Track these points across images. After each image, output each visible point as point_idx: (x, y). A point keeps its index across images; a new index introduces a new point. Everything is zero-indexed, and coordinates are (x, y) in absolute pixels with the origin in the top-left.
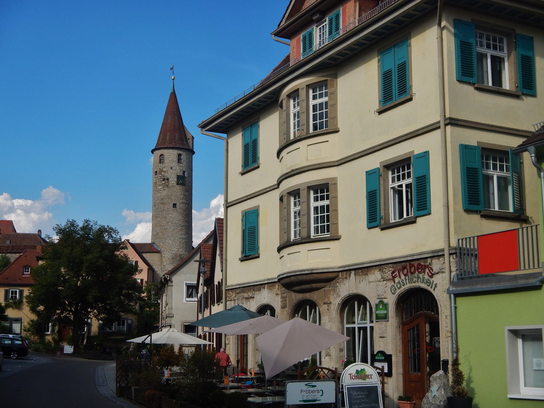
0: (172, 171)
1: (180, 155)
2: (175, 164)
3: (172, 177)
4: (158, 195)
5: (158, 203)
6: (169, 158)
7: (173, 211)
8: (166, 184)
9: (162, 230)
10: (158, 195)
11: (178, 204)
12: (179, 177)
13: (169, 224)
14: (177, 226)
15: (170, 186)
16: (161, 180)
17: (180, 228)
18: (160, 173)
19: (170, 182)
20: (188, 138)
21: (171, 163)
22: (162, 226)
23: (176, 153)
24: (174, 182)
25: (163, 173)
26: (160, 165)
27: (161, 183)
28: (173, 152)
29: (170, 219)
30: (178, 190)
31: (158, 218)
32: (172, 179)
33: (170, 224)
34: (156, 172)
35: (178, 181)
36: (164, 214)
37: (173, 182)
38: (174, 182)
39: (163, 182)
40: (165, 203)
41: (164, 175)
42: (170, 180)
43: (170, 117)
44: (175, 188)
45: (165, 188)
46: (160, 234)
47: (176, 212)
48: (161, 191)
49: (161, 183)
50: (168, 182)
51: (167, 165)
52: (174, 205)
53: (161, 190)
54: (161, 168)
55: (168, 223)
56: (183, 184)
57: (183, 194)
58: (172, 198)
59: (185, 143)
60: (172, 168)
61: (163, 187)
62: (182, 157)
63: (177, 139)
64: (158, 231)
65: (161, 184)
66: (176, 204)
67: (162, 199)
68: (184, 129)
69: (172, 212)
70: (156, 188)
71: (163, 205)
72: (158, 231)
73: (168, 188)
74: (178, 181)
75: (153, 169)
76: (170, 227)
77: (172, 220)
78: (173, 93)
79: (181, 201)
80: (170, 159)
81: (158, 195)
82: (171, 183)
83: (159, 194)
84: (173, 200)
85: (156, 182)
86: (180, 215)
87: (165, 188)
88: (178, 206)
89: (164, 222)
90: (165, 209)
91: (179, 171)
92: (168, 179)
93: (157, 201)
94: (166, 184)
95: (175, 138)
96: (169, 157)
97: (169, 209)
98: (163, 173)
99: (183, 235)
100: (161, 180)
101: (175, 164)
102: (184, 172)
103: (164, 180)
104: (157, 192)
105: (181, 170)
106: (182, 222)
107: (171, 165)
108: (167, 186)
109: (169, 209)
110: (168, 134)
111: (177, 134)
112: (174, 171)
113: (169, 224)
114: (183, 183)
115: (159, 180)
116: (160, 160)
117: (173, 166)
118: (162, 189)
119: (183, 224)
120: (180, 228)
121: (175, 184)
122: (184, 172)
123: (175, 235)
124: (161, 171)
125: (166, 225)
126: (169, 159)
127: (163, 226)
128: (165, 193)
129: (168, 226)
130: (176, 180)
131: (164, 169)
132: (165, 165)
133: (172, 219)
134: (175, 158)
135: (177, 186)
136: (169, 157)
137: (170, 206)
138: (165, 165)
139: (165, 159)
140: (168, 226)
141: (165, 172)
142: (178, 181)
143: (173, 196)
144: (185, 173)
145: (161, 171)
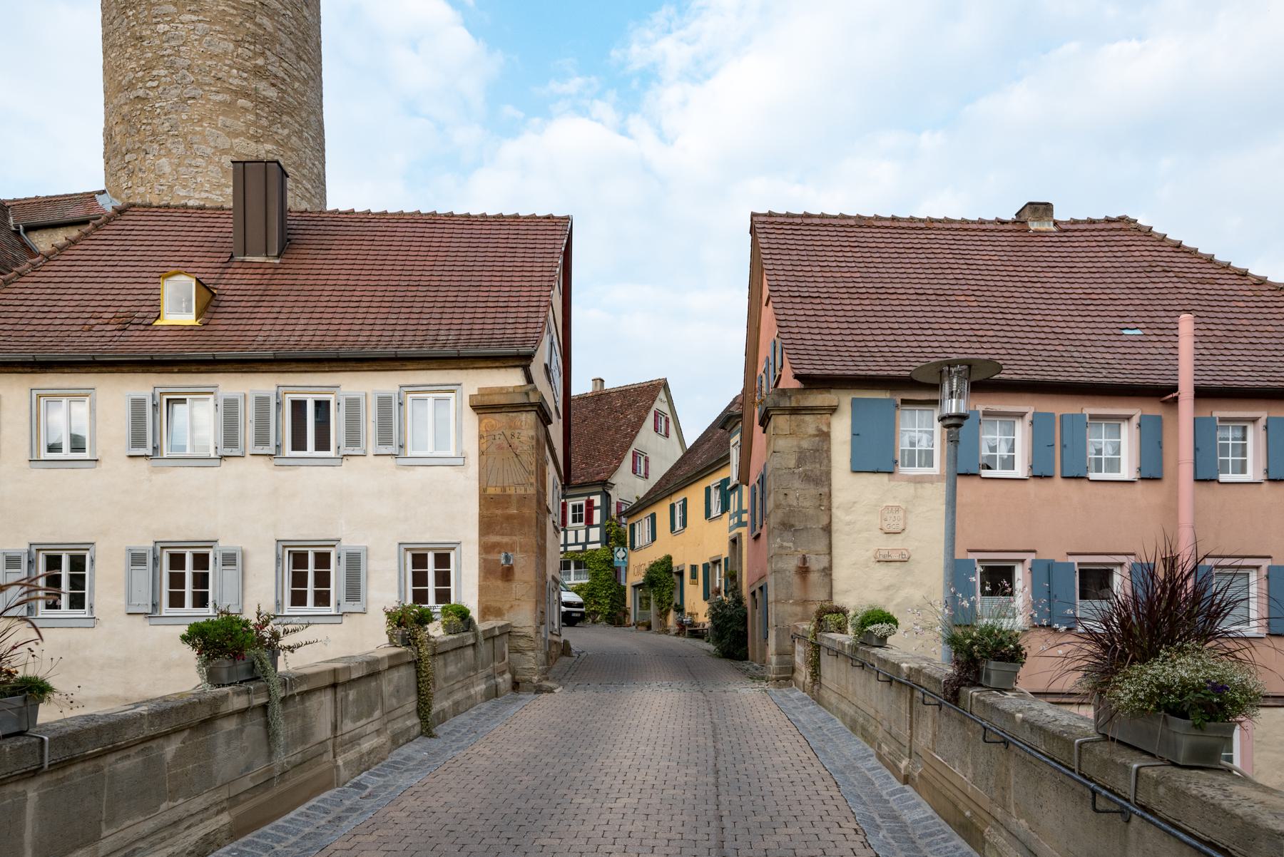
7: (175, 5)
9: (126, 109)
13: (155, 73)
14: (200, 85)
17: (219, 97)
29: (161, 48)
33: (163, 72)
46: (117, 129)
47: (192, 8)
55: (148, 68)
69: (172, 9)
76: (161, 89)
86: (218, 28)
89: (133, 65)
99: (237, 135)
106: (231, 67)
113: (155, 73)
119: (236, 82)
120: (219, 97)
123: (195, 133)
125: (142, 80)
127: (131, 86)
129: (150, 84)
133: (173, 43)
140: (150, 84)
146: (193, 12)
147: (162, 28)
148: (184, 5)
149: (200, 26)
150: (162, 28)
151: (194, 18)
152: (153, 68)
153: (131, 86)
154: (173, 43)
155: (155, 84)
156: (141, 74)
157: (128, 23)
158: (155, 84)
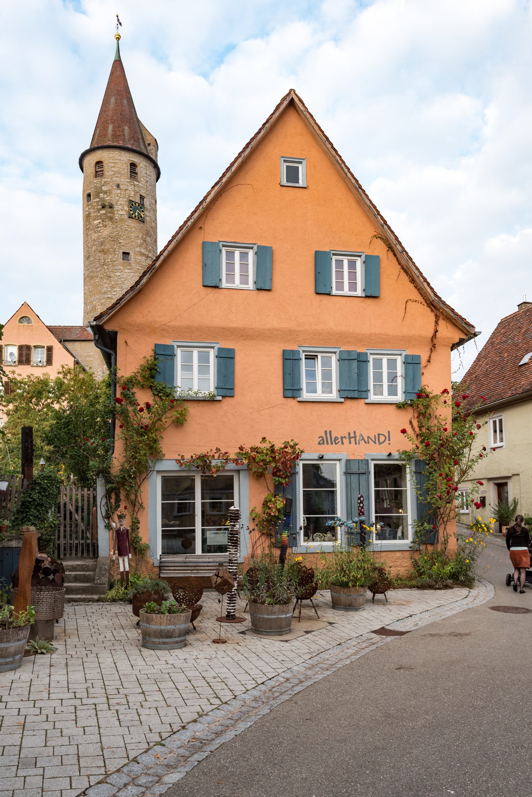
0: (119, 191)
1: (133, 165)
2: (124, 180)
3: (119, 203)
4: (94, 236)
5: (94, 252)
6: (113, 167)
8: (109, 215)
9: (103, 301)
10: (93, 237)
11: (132, 253)
12: (132, 205)
13: (115, 289)
15: (116, 219)
16: (99, 207)
18: (97, 196)
19: (116, 212)
20: (147, 143)
21: (117, 177)
22: (101, 293)
23: (125, 159)
24: (125, 213)
25: (101, 195)
26: (95, 181)
27: (99, 213)
28: (120, 157)
29: (118, 281)
30: (132, 229)
31: (95, 278)
32: (120, 207)
33: (118, 290)
34: (89, 195)
35: (131, 210)
36: (105, 270)
37: (121, 212)
38: (125, 213)
39: (103, 212)
40: (108, 251)
41: (103, 198)
42: (116, 207)
43: (113, 100)
44: (127, 223)
45: (107, 223)
46: (99, 307)
47: (129, 267)
48: (99, 229)
49: (99, 213)
50: (113, 213)
51: (109, 180)
52: (126, 254)
53: (98, 227)
54: (99, 185)
55: (113, 287)
56: (142, 220)
57: (140, 236)
58: (120, 241)
59: (142, 146)
60: (118, 186)
61: (103, 221)
62: (138, 170)
63: (127, 137)
64: (94, 302)
65: (99, 214)
66: (128, 254)
67: (102, 244)
68: (139, 124)
69: (122, 268)
70: (90, 224)
71: (104, 254)
72: (94, 302)
73: (112, 222)
74: (131, 212)
75: (84, 192)
77: (120, 282)
78: (117, 60)
79: (138, 249)
80: (114, 169)
81: (94, 236)
82: (118, 213)
83: (96, 234)
84: (123, 246)
85: (90, 213)
87: (107, 223)
88: (132, 258)
89: (107, 286)
90: (108, 262)
91: (133, 193)
92: (111, 207)
93: (92, 248)
94: (109, 215)
95: (124, 135)
96: (113, 165)
97: (115, 261)
98: (101, 195)
100: (99, 207)
101: (124, 180)
102: (142, 198)
103: (104, 207)
104: (92, 232)
105: (136, 192)
107: (117, 180)
108: (111, 219)
109: (115, 261)
110: (110, 127)
111: (126, 128)
112: (123, 192)
113: (115, 289)
114: (141, 217)
115: (94, 209)
116: (96, 172)
117: (122, 183)
118: (101, 225)
121: (126, 217)
122: (142, 198)
124: (98, 191)
126: (113, 169)
127: (105, 293)
128: (106, 232)
129: (113, 293)
130: (126, 208)
131: (103, 188)
132: (105, 180)
133: (122, 280)
134: (127, 169)
135: (130, 221)
136: (113, 165)
137: (116, 256)
138: (105, 180)
139: (105, 171)
140: (113, 293)
141: (105, 193)
142: (131, 212)
143: (122, 238)
144: (143, 200)
145: (98, 191)
146: (129, 269)
147: (118, 274)
148: (126, 267)
149: (131, 274)
150: (118, 274)
151: (129, 271)
152: (114, 288)
153: (105, 293)
154: (122, 280)
155: (115, 293)
156: (110, 289)
157: (105, 270)
158: (115, 293)
